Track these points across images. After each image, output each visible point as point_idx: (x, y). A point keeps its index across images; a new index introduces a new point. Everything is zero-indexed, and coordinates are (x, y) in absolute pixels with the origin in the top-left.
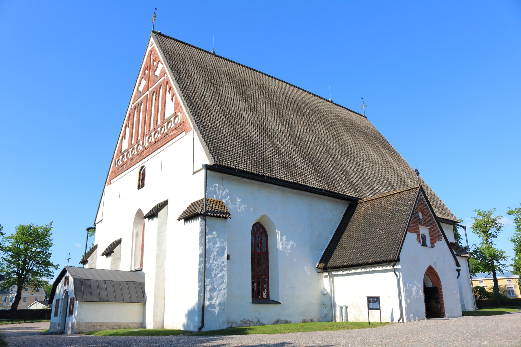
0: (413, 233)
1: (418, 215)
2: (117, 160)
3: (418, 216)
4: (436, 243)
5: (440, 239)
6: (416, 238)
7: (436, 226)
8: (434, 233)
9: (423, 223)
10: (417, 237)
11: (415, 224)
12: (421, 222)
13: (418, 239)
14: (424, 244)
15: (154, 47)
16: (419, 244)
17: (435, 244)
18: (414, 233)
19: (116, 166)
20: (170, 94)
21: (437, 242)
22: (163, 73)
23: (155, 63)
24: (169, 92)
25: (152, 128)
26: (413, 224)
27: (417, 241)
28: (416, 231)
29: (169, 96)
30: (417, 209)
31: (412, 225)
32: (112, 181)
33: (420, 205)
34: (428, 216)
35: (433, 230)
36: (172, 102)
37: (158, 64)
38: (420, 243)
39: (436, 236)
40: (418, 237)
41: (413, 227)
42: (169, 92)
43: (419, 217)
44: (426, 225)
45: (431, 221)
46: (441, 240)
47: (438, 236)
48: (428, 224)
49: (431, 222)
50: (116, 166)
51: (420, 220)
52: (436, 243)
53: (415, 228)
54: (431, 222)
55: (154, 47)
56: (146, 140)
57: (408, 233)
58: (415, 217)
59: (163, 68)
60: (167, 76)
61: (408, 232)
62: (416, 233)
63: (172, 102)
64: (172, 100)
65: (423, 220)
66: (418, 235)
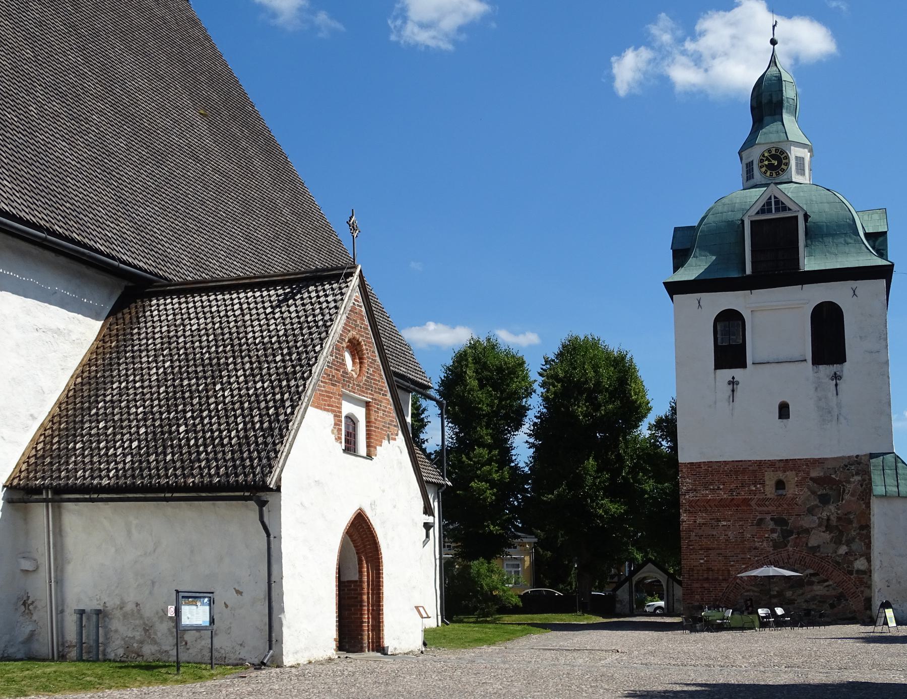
0: (325, 410)
1: (343, 360)
3: (343, 364)
4: (381, 446)
5: (391, 436)
6: (332, 427)
7: (386, 395)
8: (378, 416)
9: (354, 384)
10: (333, 422)
11: (333, 385)
12: (347, 382)
13: (335, 431)
14: (350, 447)
16: (338, 444)
17: (378, 448)
18: (328, 410)
21: (385, 442)
26: (325, 383)
27: (333, 437)
28: (332, 406)
30: (343, 340)
31: (324, 387)
33: (352, 328)
34: (368, 365)
35: (378, 409)
38: (341, 443)
39: (384, 426)
40: (335, 424)
41: (326, 392)
43: (345, 365)
44: (363, 392)
45: (375, 380)
46: (395, 439)
47: (389, 427)
48: (366, 389)
49: (374, 384)
51: (347, 373)
52: (381, 446)
53: (331, 397)
54: (374, 384)
57: (310, 408)
58: (335, 365)
61: (311, 406)
62: (332, 411)
65: (355, 376)
66: (337, 416)
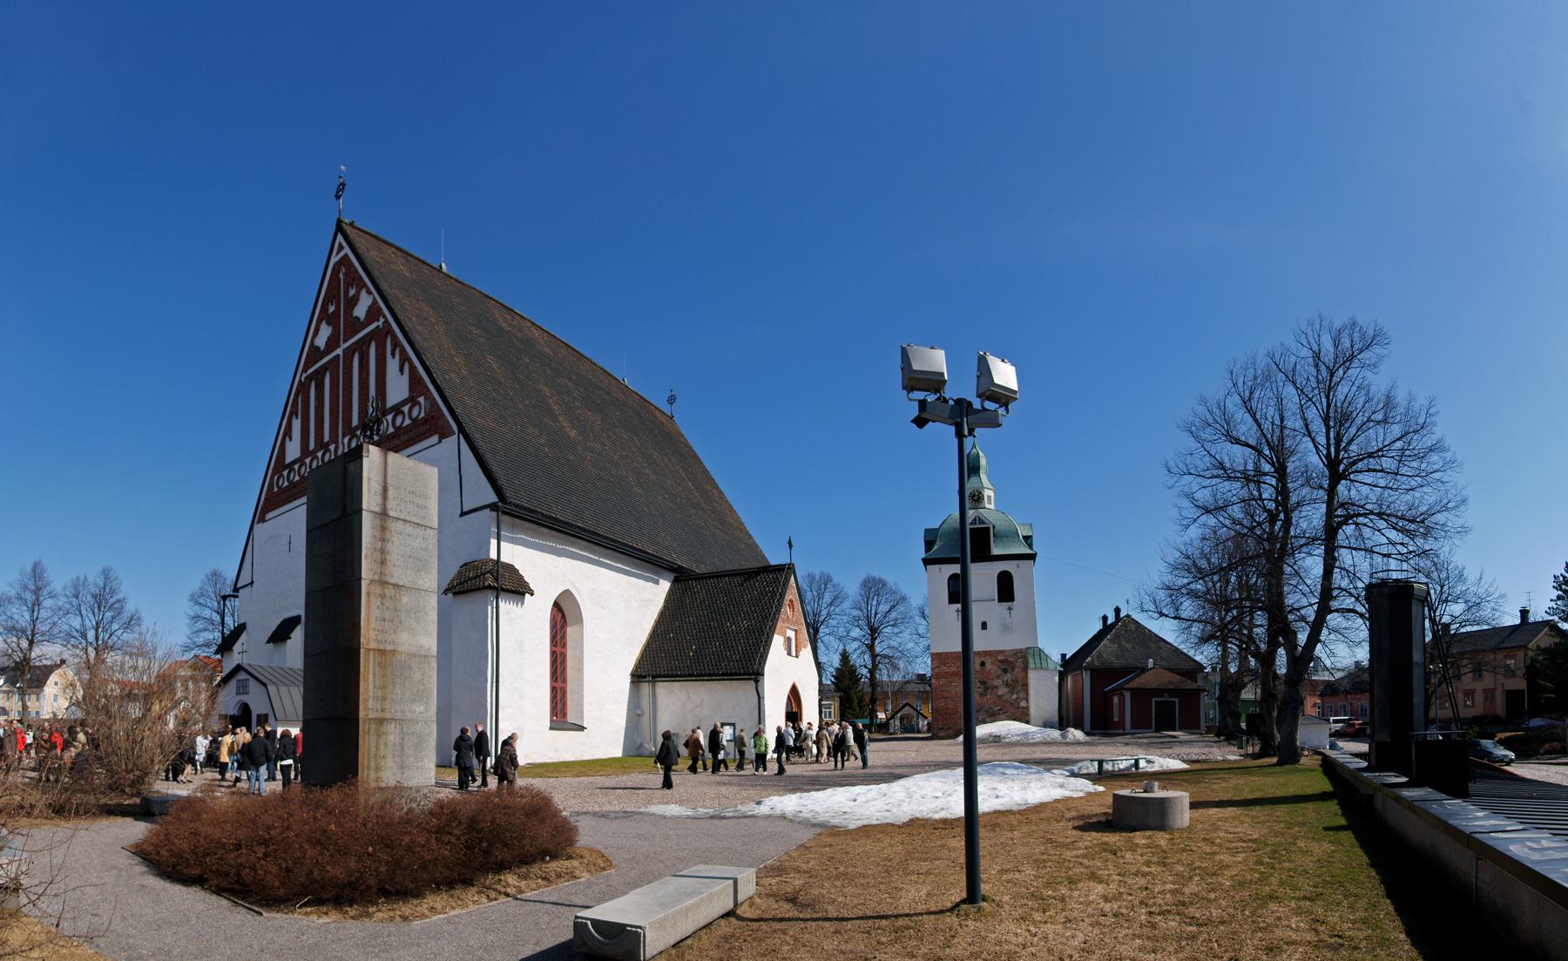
2: (276, 478)
15: (346, 255)
19: (276, 489)
20: (394, 357)
22: (373, 313)
23: (352, 292)
24: (393, 354)
25: (355, 422)
29: (392, 364)
32: (269, 516)
36: (402, 374)
37: (358, 293)
42: (393, 354)
50: (276, 489)
55: (346, 255)
56: (343, 444)
59: (375, 302)
60: (386, 321)
63: (402, 374)
64: (402, 371)
